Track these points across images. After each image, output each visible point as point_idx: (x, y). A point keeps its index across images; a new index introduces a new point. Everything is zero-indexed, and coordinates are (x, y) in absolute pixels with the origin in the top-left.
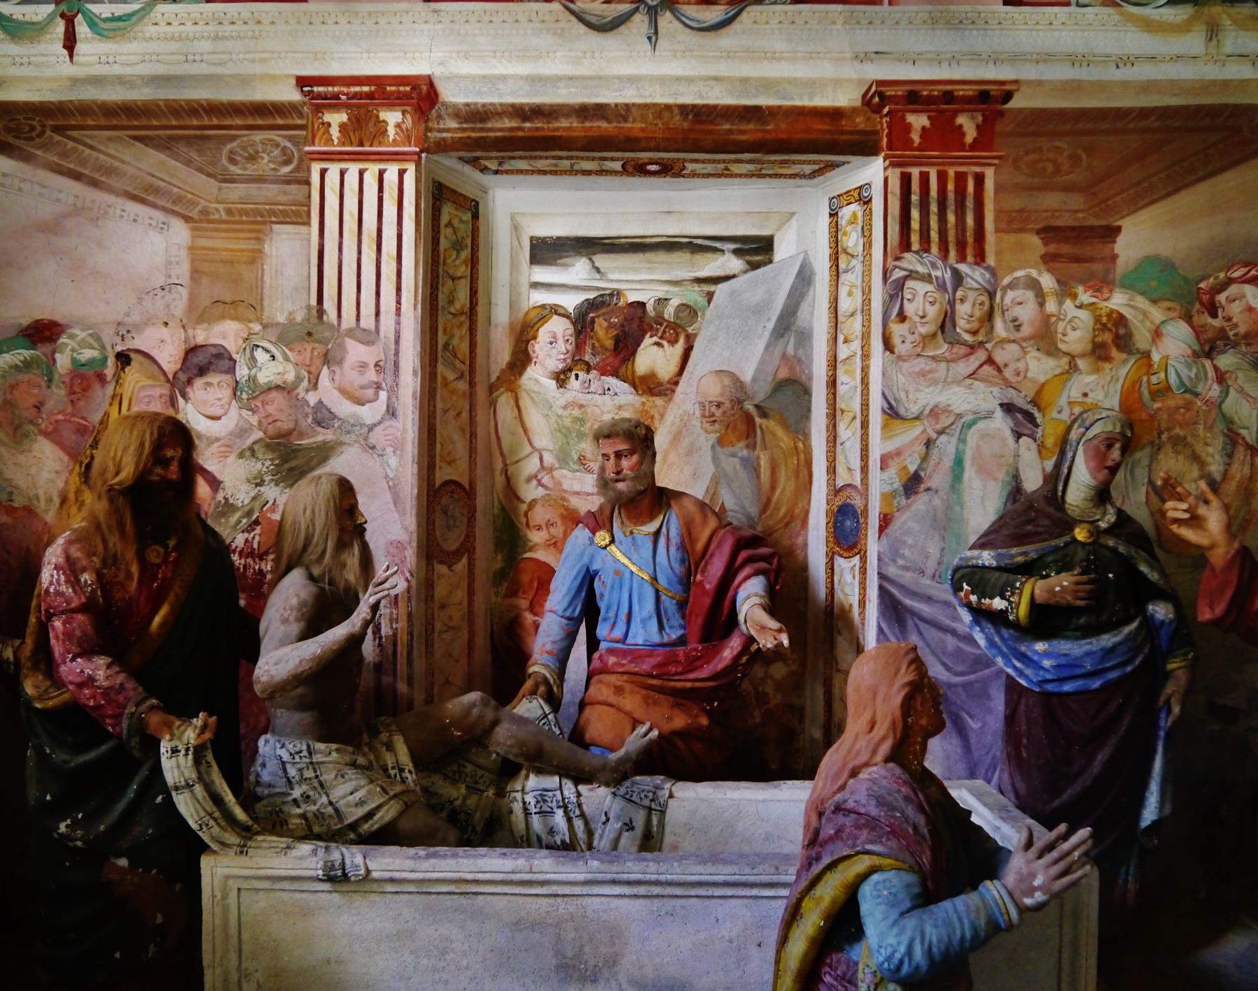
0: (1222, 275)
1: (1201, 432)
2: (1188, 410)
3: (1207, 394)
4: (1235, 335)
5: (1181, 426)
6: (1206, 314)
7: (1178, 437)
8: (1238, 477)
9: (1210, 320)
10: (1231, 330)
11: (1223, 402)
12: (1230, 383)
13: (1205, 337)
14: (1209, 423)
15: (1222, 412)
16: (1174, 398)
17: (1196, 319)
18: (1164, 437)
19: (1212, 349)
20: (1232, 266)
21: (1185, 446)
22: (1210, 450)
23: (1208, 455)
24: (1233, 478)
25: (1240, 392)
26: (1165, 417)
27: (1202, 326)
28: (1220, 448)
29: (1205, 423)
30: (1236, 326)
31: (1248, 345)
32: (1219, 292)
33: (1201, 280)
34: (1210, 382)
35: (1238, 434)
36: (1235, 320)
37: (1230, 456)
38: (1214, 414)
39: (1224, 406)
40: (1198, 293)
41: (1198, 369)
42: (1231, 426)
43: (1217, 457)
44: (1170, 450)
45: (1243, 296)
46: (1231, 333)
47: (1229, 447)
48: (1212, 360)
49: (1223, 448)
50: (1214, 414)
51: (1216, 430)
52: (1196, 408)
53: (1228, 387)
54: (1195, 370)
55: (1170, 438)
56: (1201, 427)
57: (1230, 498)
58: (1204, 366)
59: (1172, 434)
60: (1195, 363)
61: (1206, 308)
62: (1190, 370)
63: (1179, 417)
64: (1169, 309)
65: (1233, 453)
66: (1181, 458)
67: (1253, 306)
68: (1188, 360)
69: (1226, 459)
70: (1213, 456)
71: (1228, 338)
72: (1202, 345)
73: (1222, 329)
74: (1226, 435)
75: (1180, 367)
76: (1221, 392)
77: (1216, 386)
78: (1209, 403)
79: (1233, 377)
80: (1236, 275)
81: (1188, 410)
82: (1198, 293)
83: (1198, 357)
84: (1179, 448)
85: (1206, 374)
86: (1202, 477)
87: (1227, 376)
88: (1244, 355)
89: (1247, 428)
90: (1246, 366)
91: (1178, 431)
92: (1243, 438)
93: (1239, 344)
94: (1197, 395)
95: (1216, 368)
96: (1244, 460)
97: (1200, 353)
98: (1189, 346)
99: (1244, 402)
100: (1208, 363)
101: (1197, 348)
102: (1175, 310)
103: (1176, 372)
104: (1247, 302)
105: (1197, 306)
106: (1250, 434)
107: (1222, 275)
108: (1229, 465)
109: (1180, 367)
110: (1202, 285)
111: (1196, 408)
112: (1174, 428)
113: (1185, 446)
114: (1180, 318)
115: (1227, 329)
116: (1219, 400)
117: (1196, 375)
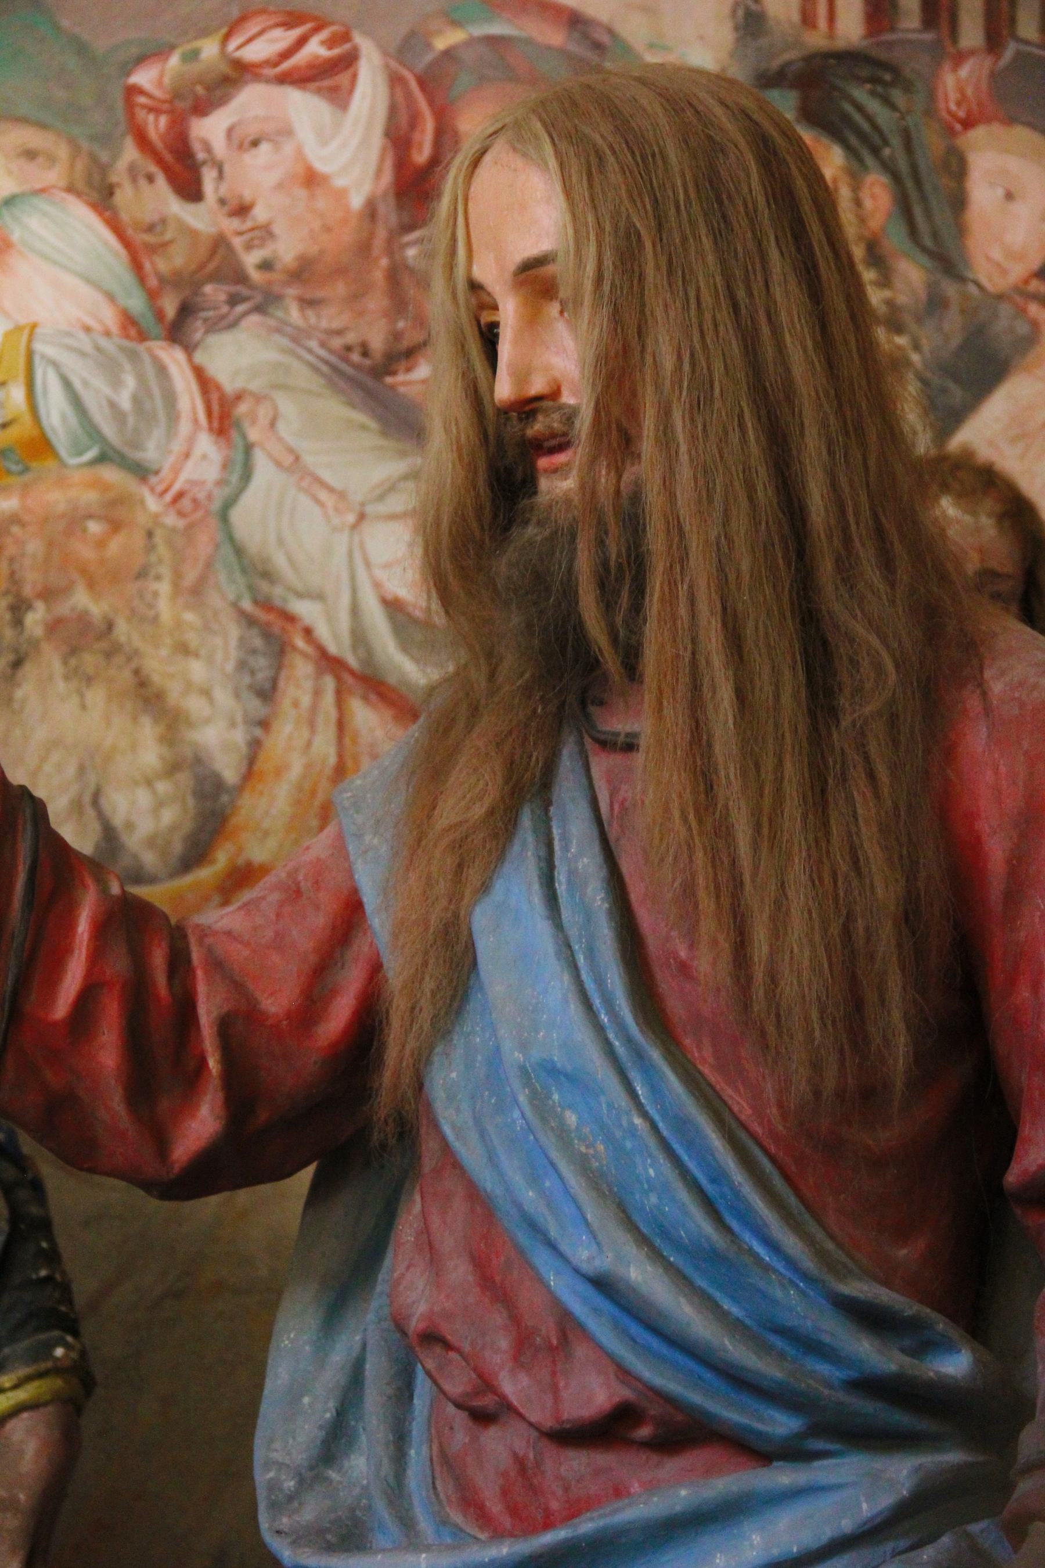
0: (209, 49)
1: (165, 608)
2: (116, 526)
3: (176, 471)
4: (266, 266)
5: (91, 585)
6: (161, 180)
7: (83, 618)
8: (296, 769)
9: (175, 207)
10: (249, 247)
11: (229, 504)
12: (254, 434)
13: (163, 265)
14: (191, 576)
15: (231, 538)
16: (62, 483)
17: (124, 196)
18: (35, 619)
19: (186, 310)
20: (243, 19)
21: (108, 655)
22: (197, 670)
23: (189, 686)
24: (279, 772)
25: (289, 470)
26: (34, 547)
27: (150, 228)
28: (230, 667)
29: (177, 576)
30: (265, 233)
31: (307, 303)
32: (202, 108)
33: (141, 60)
34: (185, 427)
35: (290, 618)
36: (260, 214)
37: (267, 693)
38: (204, 543)
39: (236, 515)
40: (130, 106)
41: (141, 378)
42: (264, 586)
43: (223, 697)
44: (57, 666)
45: (287, 132)
46: (250, 260)
47: (261, 662)
48: (189, 349)
49: (242, 665)
50: (204, 543)
51: (214, 600)
52: (142, 519)
53: (248, 449)
54: (130, 382)
55: (53, 626)
56: (164, 588)
57: (272, 843)
58: (162, 370)
59: (63, 609)
60: (133, 356)
61: (160, 161)
62: (116, 383)
63: (86, 553)
64: (30, 155)
65: (274, 682)
66: (96, 696)
67: (321, 167)
68: (103, 342)
69: (256, 707)
70: (206, 693)
71: (240, 277)
72: (152, 296)
73: (220, 243)
74: (250, 621)
75: (79, 370)
76: (226, 466)
77: (206, 444)
78: (186, 503)
79: (263, 413)
80: (258, 51)
81: (116, 526)
82: (130, 106)
83: (143, 336)
84: (90, 660)
85: (170, 398)
86: (172, 769)
87: (242, 408)
88: (295, 340)
89: (319, 596)
90: (303, 376)
91: (81, 599)
92: (308, 632)
93: (279, 298)
94: (142, 472)
95: (204, 381)
96: (314, 708)
97: (148, 321)
98: (111, 297)
99: (304, 500)
100: (174, 359)
101: (136, 303)
102: (52, 160)
103: (67, 384)
104: (300, 154)
105: (130, 153)
106: (331, 619)
107: (209, 49)
108: (264, 724)
109: (79, 370)
110: (144, 78)
111: (142, 519)
112: (67, 590)
113: (108, 655)
114: (70, 189)
115: (237, 242)
116: (220, 495)
117: (136, 400)
